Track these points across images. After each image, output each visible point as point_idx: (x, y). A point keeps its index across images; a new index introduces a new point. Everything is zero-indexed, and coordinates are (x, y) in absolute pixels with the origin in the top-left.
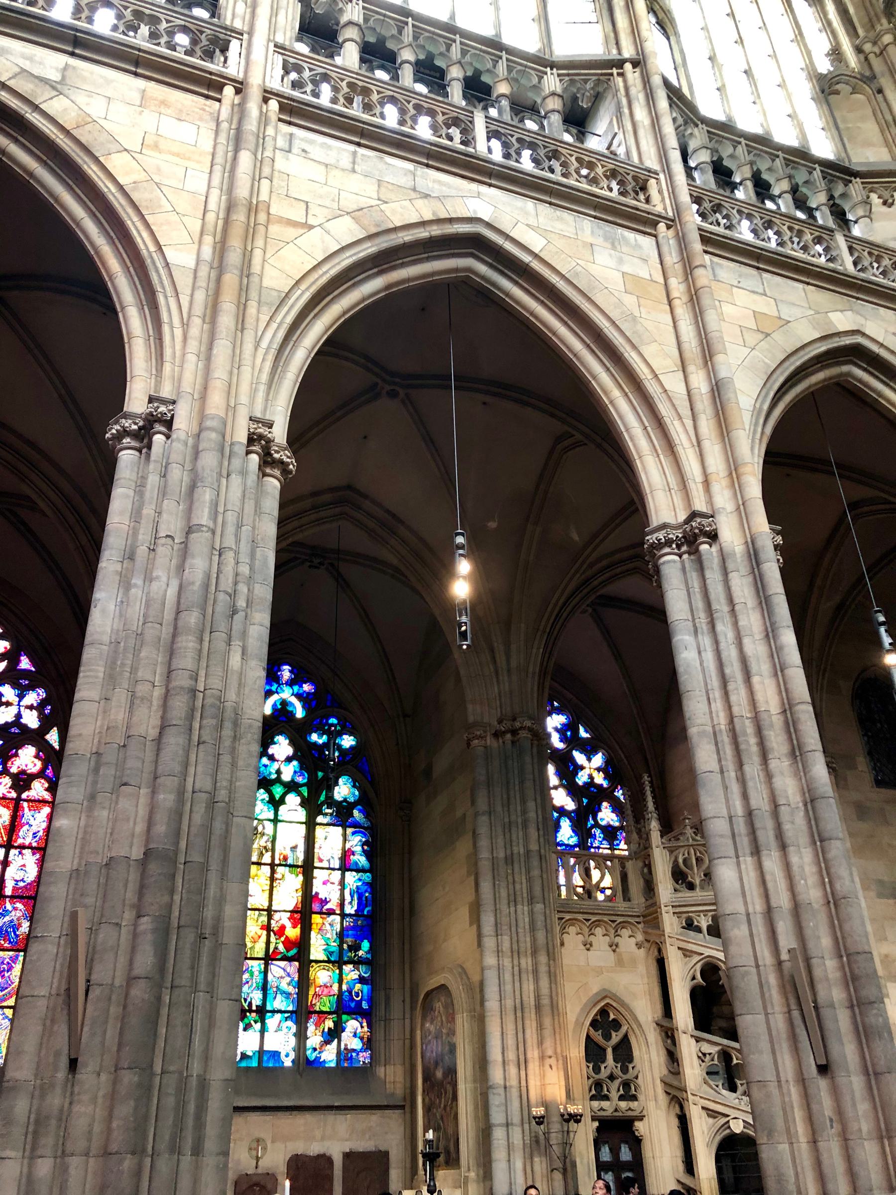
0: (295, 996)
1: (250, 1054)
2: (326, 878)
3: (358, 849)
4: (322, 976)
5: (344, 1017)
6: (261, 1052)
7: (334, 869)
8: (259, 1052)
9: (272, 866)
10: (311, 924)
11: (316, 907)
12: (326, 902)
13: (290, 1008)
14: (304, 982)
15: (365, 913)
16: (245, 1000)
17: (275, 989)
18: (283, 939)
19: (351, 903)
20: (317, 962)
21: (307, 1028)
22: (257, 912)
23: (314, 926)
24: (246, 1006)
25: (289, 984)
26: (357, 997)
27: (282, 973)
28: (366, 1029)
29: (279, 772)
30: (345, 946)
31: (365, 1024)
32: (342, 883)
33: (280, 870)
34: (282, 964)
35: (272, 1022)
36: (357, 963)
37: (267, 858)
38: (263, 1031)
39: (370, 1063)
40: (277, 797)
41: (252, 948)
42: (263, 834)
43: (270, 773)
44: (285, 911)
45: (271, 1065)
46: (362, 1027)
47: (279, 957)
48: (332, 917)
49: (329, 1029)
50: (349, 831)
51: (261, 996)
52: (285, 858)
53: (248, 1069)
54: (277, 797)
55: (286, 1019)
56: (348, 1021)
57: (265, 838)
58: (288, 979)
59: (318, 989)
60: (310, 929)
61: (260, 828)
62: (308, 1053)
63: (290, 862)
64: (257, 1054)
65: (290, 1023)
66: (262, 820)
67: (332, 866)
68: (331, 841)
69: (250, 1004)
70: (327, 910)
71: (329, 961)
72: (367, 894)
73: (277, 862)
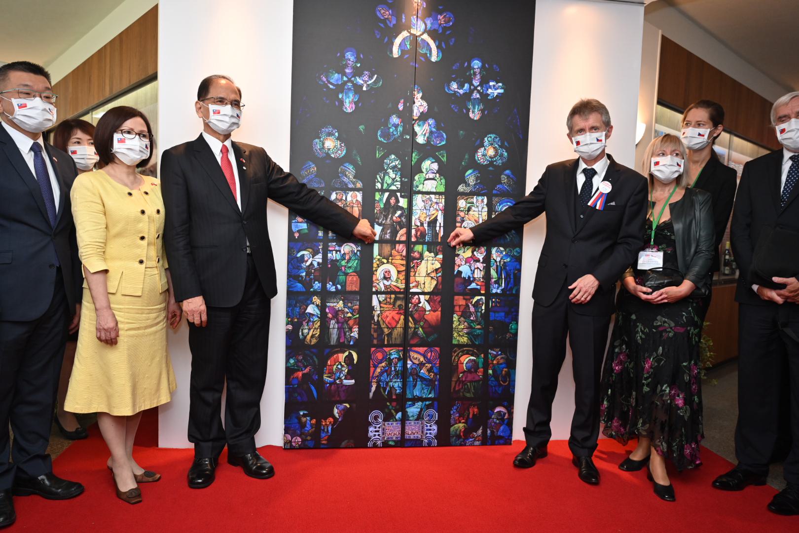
9: (409, 244)
10: (454, 306)
12: (469, 281)
14: (447, 367)
16: (385, 389)
18: (422, 323)
19: (497, 282)
20: (460, 346)
22: (393, 296)
23: (457, 309)
26: (504, 382)
27: (422, 359)
32: (487, 260)
33: (418, 248)
34: (422, 350)
37: (401, 235)
38: (405, 419)
41: (390, 335)
44: (423, 293)
50: (495, 199)
52: (423, 235)
55: (428, 407)
57: (399, 213)
58: (429, 366)
61: (393, 201)
65: (432, 411)
66: (395, 191)
73: (413, 239)
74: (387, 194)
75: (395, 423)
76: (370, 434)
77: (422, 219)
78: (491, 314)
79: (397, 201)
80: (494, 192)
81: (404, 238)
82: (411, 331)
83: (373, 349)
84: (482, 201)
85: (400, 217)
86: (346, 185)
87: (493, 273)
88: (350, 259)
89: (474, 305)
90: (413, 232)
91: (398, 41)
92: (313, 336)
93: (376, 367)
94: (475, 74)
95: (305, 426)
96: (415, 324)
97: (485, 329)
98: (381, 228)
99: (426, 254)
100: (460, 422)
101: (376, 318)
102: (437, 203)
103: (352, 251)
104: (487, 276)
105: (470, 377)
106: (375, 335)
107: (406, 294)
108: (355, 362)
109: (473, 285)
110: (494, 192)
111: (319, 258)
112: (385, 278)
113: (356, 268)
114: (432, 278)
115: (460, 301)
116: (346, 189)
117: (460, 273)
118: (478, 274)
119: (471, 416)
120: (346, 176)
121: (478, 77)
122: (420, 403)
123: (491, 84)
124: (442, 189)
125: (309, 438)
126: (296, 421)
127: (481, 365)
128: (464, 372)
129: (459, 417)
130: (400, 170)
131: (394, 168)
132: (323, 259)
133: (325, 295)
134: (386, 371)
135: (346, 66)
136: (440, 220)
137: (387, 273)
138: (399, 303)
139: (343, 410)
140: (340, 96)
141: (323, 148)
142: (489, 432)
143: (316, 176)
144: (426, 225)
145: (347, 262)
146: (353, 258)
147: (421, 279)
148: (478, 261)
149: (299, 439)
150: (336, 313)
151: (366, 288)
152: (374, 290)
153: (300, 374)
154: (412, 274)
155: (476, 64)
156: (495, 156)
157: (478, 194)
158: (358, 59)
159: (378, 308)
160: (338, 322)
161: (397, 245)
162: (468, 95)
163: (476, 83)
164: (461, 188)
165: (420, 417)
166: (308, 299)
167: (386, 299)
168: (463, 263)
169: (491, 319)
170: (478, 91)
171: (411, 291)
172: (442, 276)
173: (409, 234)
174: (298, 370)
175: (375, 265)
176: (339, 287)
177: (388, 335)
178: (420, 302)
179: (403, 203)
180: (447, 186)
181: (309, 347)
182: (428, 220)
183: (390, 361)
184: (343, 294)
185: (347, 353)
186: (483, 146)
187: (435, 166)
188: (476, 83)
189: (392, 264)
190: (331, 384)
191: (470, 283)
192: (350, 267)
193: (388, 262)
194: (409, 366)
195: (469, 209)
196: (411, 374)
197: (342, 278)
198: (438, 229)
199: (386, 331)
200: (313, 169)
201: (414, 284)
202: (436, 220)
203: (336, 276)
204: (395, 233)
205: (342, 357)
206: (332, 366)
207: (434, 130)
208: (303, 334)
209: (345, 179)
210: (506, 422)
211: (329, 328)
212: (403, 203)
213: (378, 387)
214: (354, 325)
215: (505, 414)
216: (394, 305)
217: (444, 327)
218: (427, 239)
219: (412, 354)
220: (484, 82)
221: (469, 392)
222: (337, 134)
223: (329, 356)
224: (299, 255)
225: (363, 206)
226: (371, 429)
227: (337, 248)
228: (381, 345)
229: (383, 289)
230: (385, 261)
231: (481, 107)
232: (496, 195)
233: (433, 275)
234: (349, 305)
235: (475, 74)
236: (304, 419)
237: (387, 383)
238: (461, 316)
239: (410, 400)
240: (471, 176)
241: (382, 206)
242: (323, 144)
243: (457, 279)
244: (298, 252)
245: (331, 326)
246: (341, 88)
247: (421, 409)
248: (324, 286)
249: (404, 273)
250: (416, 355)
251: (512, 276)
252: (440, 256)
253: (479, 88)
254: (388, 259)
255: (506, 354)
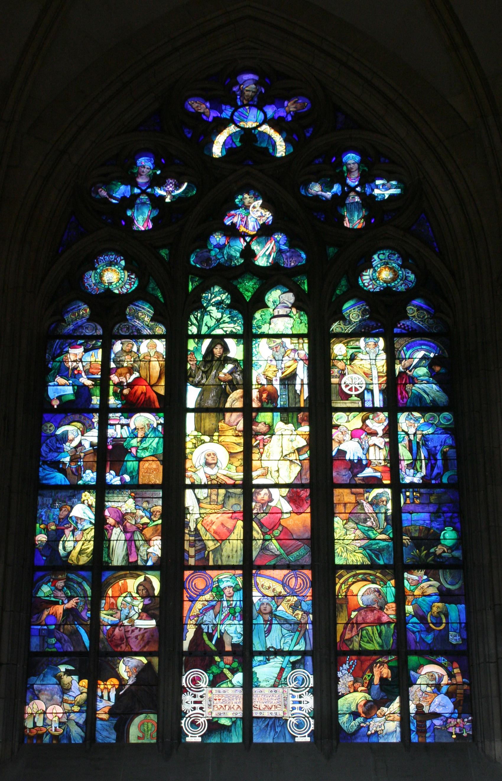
0: (309, 627)
1: (227, 723)
2: (359, 425)
3: (422, 371)
4: (361, 592)
5: (413, 660)
6: (248, 718)
7: (374, 410)
8: (243, 719)
9: (248, 413)
11: (340, 474)
12: (358, 465)
13: (301, 647)
15: (445, 480)
16: (210, 636)
17: (268, 617)
18: (276, 533)
19: (412, 466)
20: (349, 568)
21: (337, 680)
22: (222, 491)
23: (339, 509)
24: (212, 645)
25: (295, 607)
27: (279, 589)
28: (459, 679)
29: (248, 254)
30: (406, 539)
31: (456, 671)
32: (392, 431)
33: (265, 417)
34: (279, 574)
35: (265, 671)
36: (432, 567)
37: (235, 399)
39: (473, 737)
40: (248, 296)
42: (225, 360)
43: (231, 258)
44: (277, 486)
45: (269, 740)
46: (451, 676)
47: (273, 563)
48: (376, 492)
49: (382, 679)
50: (399, 343)
51: (240, 629)
53: (223, 747)
54: (248, 296)
55: (294, 665)
56: (421, 666)
57: (229, 367)
59: (354, 614)
60: (332, 515)
61: (218, 351)
62: (343, 720)
63: (280, 403)
64: (239, 723)
65: (301, 672)
66: (221, 338)
67: (368, 404)
68: (362, 365)
69: (220, 642)
70: (365, 478)
71: (373, 566)
72: (446, 449)
73: (255, 405)
74: (207, 342)
75: (230, 691)
76: (185, 707)
77: (270, 374)
78: (404, 516)
79: (226, 349)
80: (396, 330)
81: (239, 404)
82: (257, 545)
83: (187, 573)
84: (376, 345)
85: (231, 373)
86: (139, 330)
87: (404, 453)
88: (145, 437)
89: (371, 504)
90: (255, 393)
91: (221, 139)
92: (81, 552)
93: (193, 600)
94: (349, 171)
95: (69, 690)
96: (264, 534)
97: (397, 540)
98: (199, 390)
99: (279, 426)
100: (355, 691)
101: (192, 526)
102: (295, 350)
103: (149, 425)
104: (394, 458)
105: (371, 617)
106: (192, 552)
107: (248, 487)
108: (157, 592)
109: (368, 472)
110: (396, 330)
111: (93, 436)
112: (207, 464)
113: (156, 449)
114: (291, 461)
115: (343, 496)
116: (137, 336)
117: (342, 453)
118: (379, 455)
119: (376, 681)
120: (138, 318)
121: (356, 174)
122: (279, 659)
123: (378, 182)
124: (304, 330)
125: (76, 709)
126: (55, 680)
127: (391, 598)
128: (359, 609)
129: (355, 681)
130: (229, 306)
131: (218, 305)
132: (99, 437)
133: (102, 489)
134: (213, 607)
135: (139, 174)
136: (302, 374)
137: (210, 456)
138: (232, 501)
139: (136, 667)
140: (129, 213)
141: (101, 282)
142: (413, 708)
143: (88, 320)
144: (277, 384)
145: (141, 441)
146: (151, 435)
147: (273, 466)
148: (375, 434)
149: (59, 709)
150: (122, 519)
151: (174, 482)
152: (188, 482)
153: (59, 609)
154: (255, 456)
155: (352, 159)
156: (393, 280)
157: (368, 335)
158: (156, 166)
159: (196, 510)
160: (125, 531)
161: (228, 415)
162: (339, 201)
163: (352, 182)
164: (336, 327)
165: (279, 681)
166: (74, 496)
167: (209, 496)
168: (348, 437)
169: (405, 524)
170: (357, 192)
171: (255, 482)
172: (311, 459)
173: (247, 397)
174: (57, 603)
175: (189, 445)
176: (127, 478)
177: (214, 551)
178: (271, 500)
179: (236, 350)
180: (311, 325)
181: (78, 569)
182: (279, 375)
183: (220, 592)
184: (136, 488)
185: (141, 579)
186: (371, 266)
187: (290, 298)
188: (352, 182)
189: (219, 442)
190: (114, 626)
191: (363, 468)
192: (146, 449)
193: (212, 441)
194: (255, 600)
195: (352, 358)
196: (260, 612)
197: (131, 464)
198: (298, 387)
199: (211, 545)
200: (85, 310)
201: (259, 472)
202: (293, 376)
203: (122, 461)
204: (224, 395)
205: (132, 584)
206: (115, 597)
207: (284, 247)
208: (64, 548)
209: (137, 323)
210: (444, 689)
211: (109, 540)
212: (236, 350)
213: (199, 631)
214: (153, 535)
215: (441, 678)
216: (223, 505)
217: (321, 539)
218: (280, 403)
219: (260, 580)
220: (367, 179)
221: (370, 641)
222: (123, 263)
223: (108, 585)
224: (59, 432)
225: (166, 360)
226: (187, 698)
227: (124, 421)
228: (203, 567)
229: (204, 481)
230: (207, 438)
231: (363, 213)
232: (400, 335)
233: (293, 457)
234: (145, 505)
235: (349, 171)
236: (66, 679)
237: (215, 626)
238: (348, 520)
239: (260, 653)
240: (353, 312)
241: (200, 358)
242: (101, 277)
243: (335, 463)
244: (57, 427)
245: (114, 537)
246: (130, 202)
247: (282, 670)
248: (101, 477)
249: (241, 456)
250: (267, 583)
251: (439, 457)
252: (305, 429)
253: (358, 189)
254: (211, 436)
255: (438, 580)
